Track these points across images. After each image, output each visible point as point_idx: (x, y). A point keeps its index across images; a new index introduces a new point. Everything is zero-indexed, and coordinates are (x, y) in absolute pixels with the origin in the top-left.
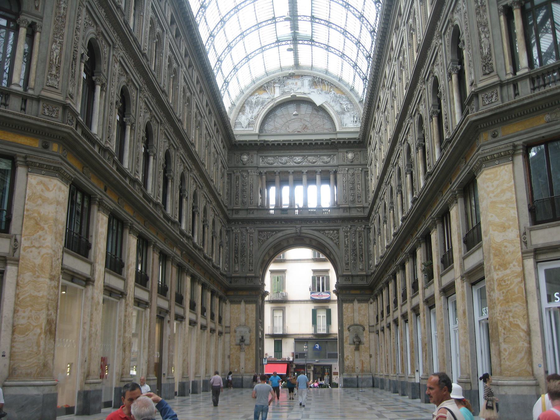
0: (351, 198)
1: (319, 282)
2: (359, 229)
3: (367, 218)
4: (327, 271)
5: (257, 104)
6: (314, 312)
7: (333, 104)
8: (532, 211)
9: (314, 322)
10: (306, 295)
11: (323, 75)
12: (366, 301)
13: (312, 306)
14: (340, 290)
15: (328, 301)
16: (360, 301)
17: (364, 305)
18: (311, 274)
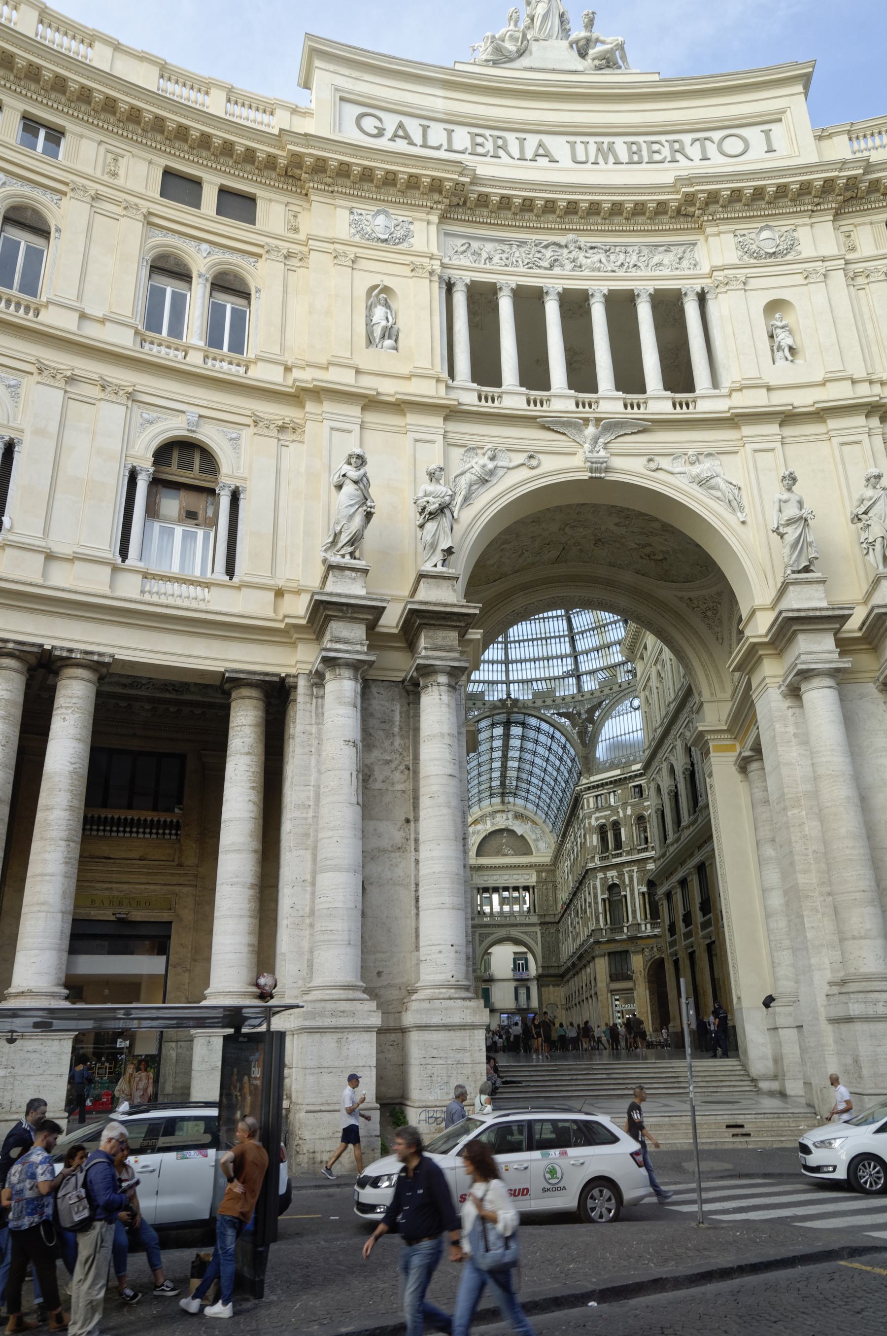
0: (545, 908)
1: (519, 963)
2: (552, 931)
3: (559, 922)
4: (525, 953)
5: (474, 833)
6: (516, 989)
7: (530, 833)
8: (610, 976)
9: (517, 998)
10: (509, 974)
11: (522, 810)
12: (558, 985)
13: (513, 984)
14: (539, 978)
15: (527, 980)
16: (554, 986)
17: (557, 988)
18: (512, 956)
